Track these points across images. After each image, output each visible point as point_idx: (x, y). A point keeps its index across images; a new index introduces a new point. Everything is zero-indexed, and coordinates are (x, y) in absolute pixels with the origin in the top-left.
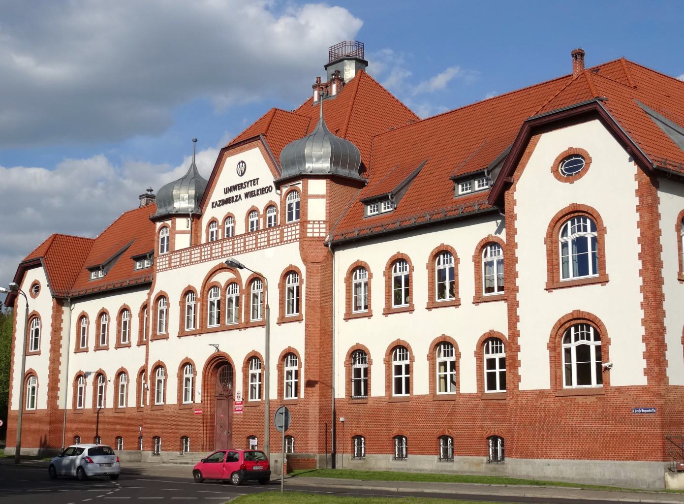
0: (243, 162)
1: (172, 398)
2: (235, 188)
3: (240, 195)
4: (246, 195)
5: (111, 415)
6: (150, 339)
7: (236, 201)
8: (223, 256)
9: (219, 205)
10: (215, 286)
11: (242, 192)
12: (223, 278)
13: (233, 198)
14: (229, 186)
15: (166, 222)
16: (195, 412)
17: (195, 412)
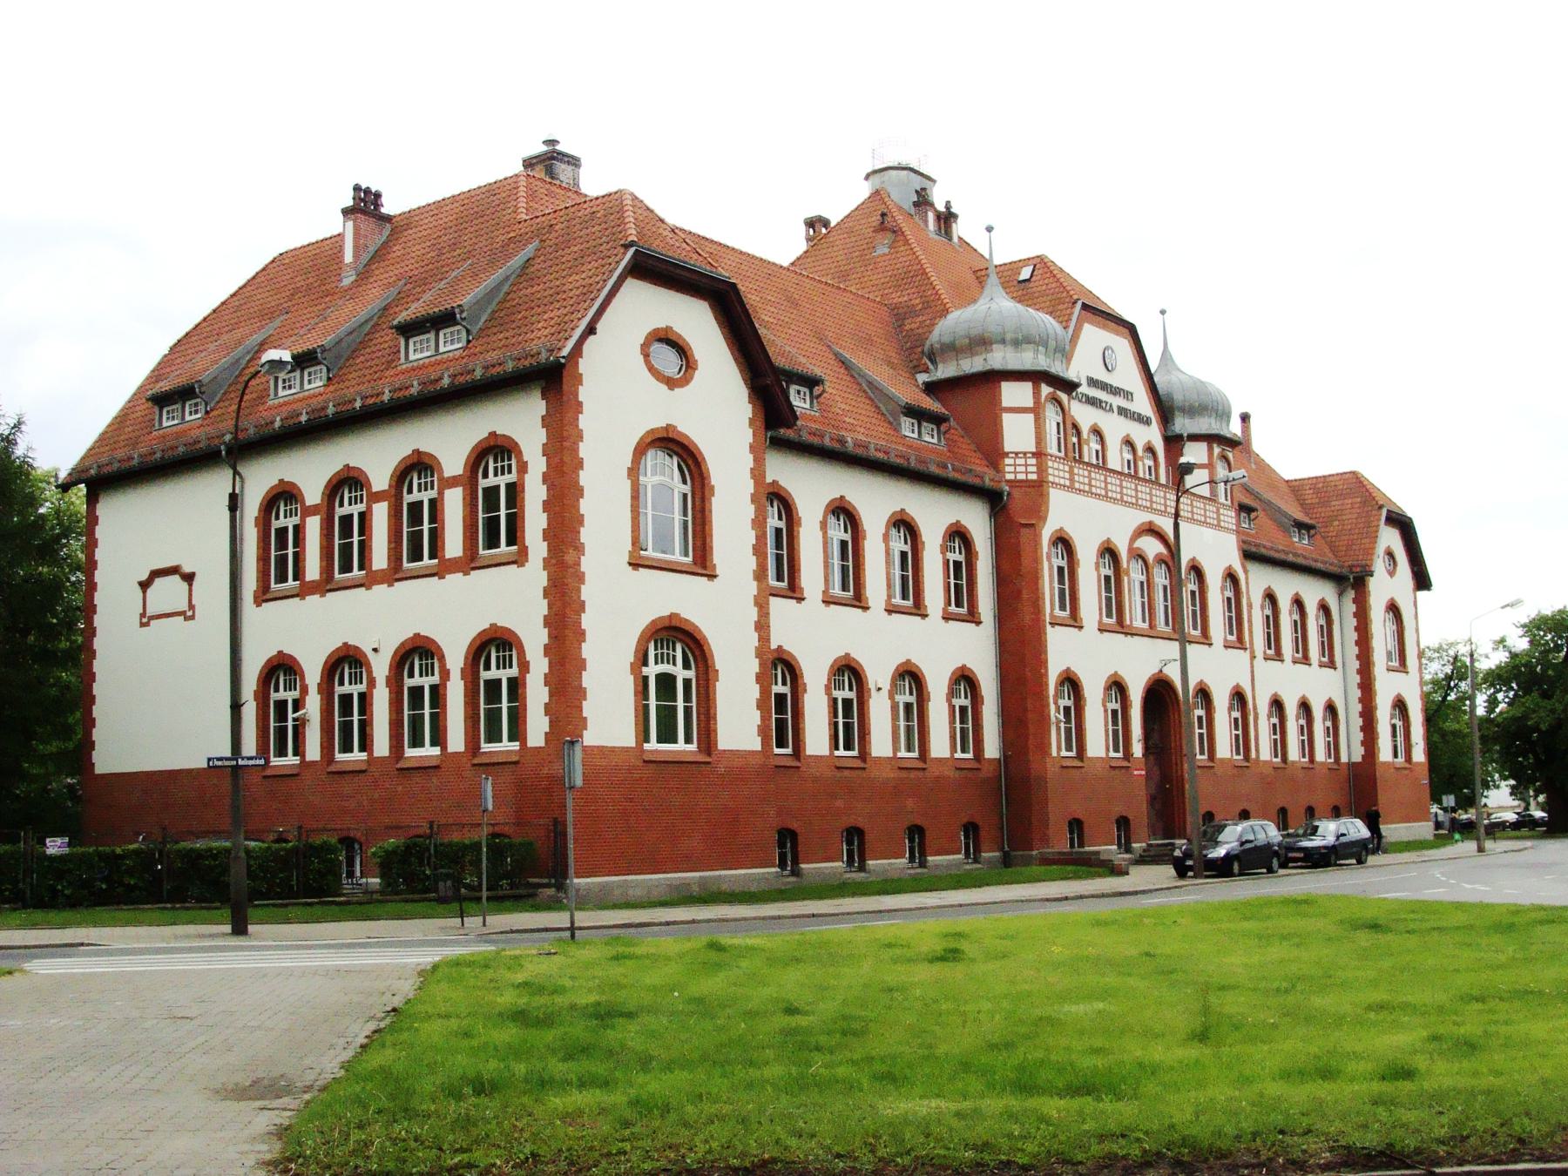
0: (1113, 351)
1: (1097, 744)
2: (1104, 386)
3: (1111, 406)
4: (1123, 412)
5: (889, 774)
6: (1048, 620)
7: (1104, 409)
8: (1151, 509)
9: (1080, 401)
10: (1140, 556)
11: (1117, 401)
12: (1152, 547)
13: (1101, 401)
14: (1095, 377)
15: (1059, 393)
16: (1136, 773)
17: (1136, 773)
